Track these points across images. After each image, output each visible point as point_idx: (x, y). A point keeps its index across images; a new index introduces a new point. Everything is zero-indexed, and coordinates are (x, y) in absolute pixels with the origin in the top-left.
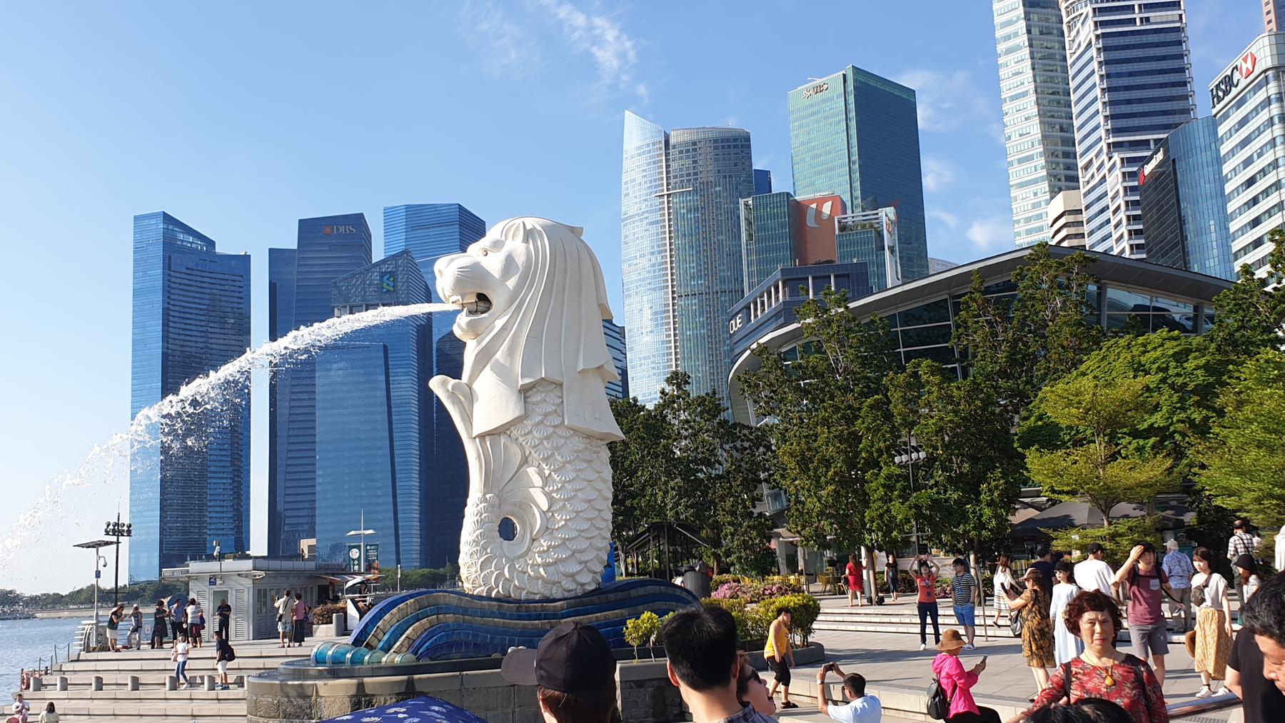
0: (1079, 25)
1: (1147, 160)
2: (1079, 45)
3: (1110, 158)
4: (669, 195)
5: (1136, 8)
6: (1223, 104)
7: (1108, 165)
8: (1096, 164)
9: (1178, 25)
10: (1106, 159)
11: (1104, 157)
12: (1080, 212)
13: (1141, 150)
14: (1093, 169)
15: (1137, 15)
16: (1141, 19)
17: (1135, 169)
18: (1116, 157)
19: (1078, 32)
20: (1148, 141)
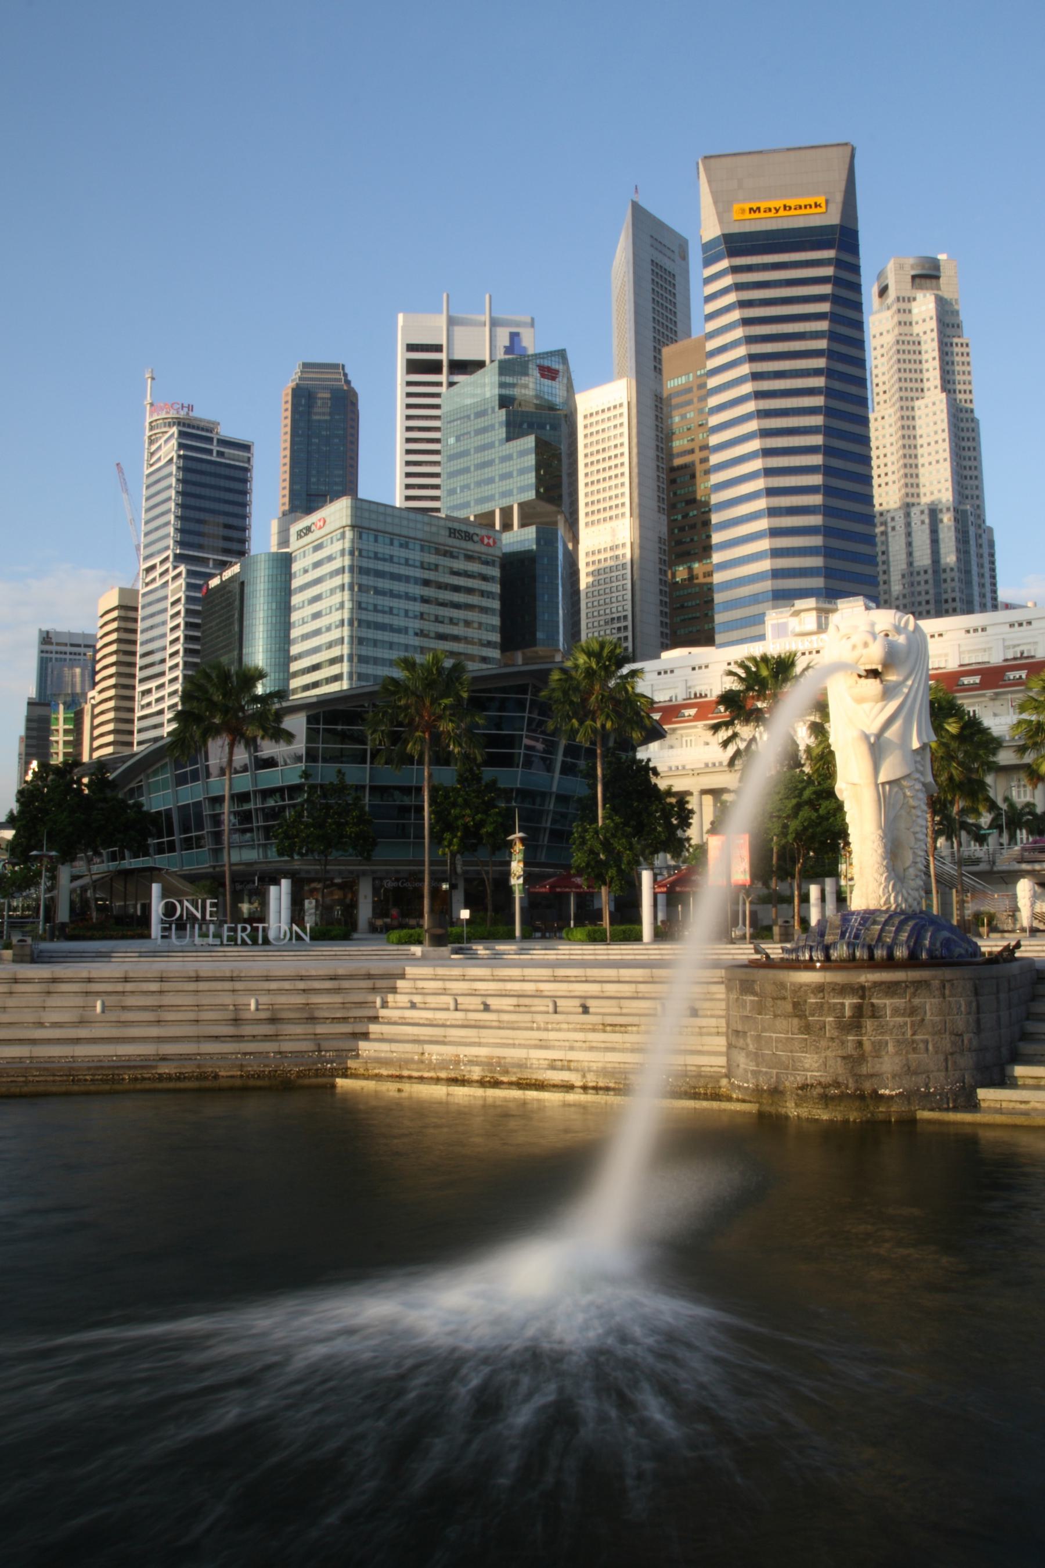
0: (162, 441)
1: (212, 576)
2: (159, 459)
3: (175, 568)
7: (172, 574)
8: (160, 570)
9: (246, 465)
11: (169, 565)
13: (202, 566)
14: (155, 574)
15: (215, 448)
16: (218, 452)
17: (201, 582)
18: (182, 568)
19: (159, 448)
20: (208, 559)
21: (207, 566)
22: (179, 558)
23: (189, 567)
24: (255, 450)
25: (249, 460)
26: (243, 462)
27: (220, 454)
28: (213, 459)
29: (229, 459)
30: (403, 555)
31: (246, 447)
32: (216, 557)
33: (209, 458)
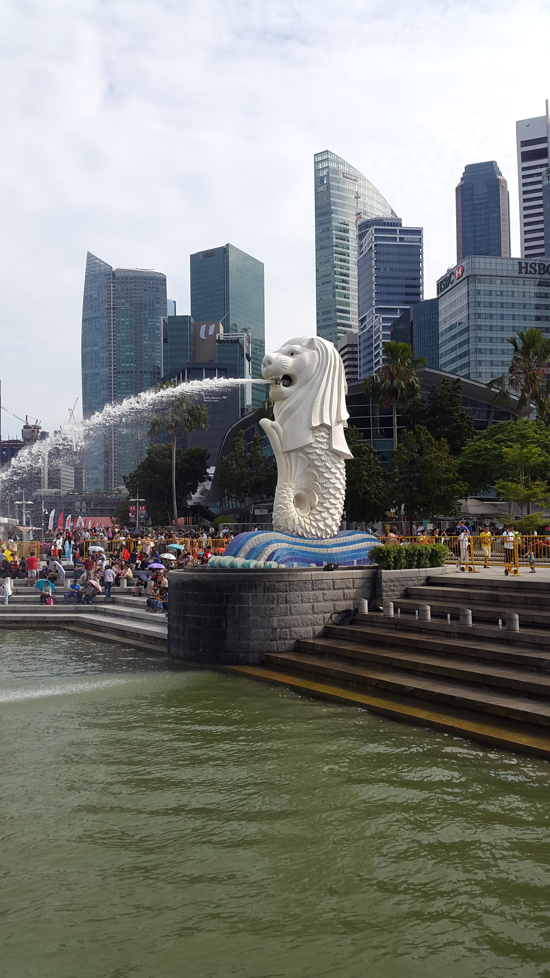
3: (376, 317)
4: (114, 309)
5: (398, 231)
6: (443, 293)
9: (419, 244)
10: (374, 317)
12: (356, 346)
17: (390, 324)
20: (397, 309)
21: (397, 314)
22: (378, 310)
23: (383, 316)
24: (424, 233)
25: (420, 240)
26: (417, 242)
27: (402, 239)
28: (397, 243)
29: (407, 242)
30: (509, 289)
31: (418, 232)
32: (401, 307)
33: (394, 243)
